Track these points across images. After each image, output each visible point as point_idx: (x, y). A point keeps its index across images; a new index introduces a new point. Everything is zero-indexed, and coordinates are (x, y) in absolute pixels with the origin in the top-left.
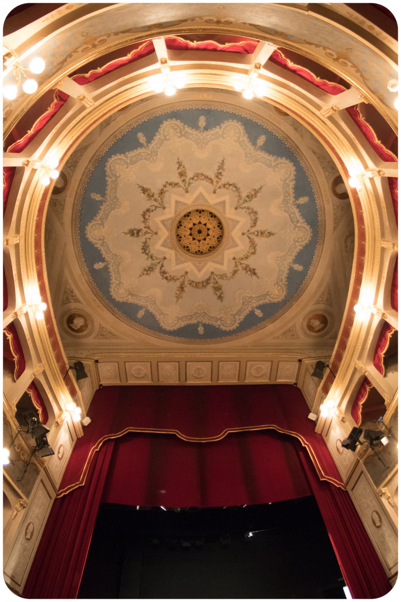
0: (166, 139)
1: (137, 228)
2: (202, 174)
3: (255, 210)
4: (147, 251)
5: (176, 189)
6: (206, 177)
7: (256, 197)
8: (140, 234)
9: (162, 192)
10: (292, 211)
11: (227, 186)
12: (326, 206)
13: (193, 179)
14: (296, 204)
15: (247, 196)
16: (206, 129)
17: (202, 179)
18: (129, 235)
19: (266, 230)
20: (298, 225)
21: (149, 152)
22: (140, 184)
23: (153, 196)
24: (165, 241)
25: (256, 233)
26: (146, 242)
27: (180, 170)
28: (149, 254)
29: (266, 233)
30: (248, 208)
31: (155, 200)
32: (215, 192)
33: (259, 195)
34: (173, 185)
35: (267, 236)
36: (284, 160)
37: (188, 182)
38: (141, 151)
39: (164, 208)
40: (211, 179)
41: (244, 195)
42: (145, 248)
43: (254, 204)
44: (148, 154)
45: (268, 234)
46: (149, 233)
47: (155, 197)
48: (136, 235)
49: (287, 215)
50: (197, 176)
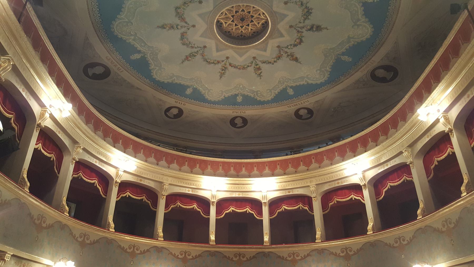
0: (270, 90)
1: (312, 32)
2: (240, 69)
3: (185, 47)
4: (306, 10)
5: (265, 59)
6: (235, 67)
7: (187, 56)
8: (309, 27)
9: (279, 57)
10: (144, 48)
11: (215, 62)
12: (109, 55)
13: (248, 66)
14: (142, 53)
15: (195, 56)
16: (236, 95)
17: (240, 66)
18: (322, 27)
19: (168, 30)
20: (133, 37)
21: (285, 83)
22: (299, 64)
23: (288, 55)
24: (283, 20)
25: (179, 27)
26: (305, 19)
27: (260, 71)
28: (304, 7)
29: (168, 28)
30: (192, 47)
31: (286, 52)
32: (227, 58)
33: (184, 57)
34: (267, 62)
35: (166, 25)
36: (166, 81)
37: (253, 64)
38: (292, 84)
39: (278, 47)
40: (232, 66)
41: (198, 57)
42: (308, 13)
43: (188, 51)
44: (287, 82)
45: (165, 27)
46: (299, 27)
47: (286, 54)
48: (315, 27)
49: (149, 44)
50: (244, 68)
